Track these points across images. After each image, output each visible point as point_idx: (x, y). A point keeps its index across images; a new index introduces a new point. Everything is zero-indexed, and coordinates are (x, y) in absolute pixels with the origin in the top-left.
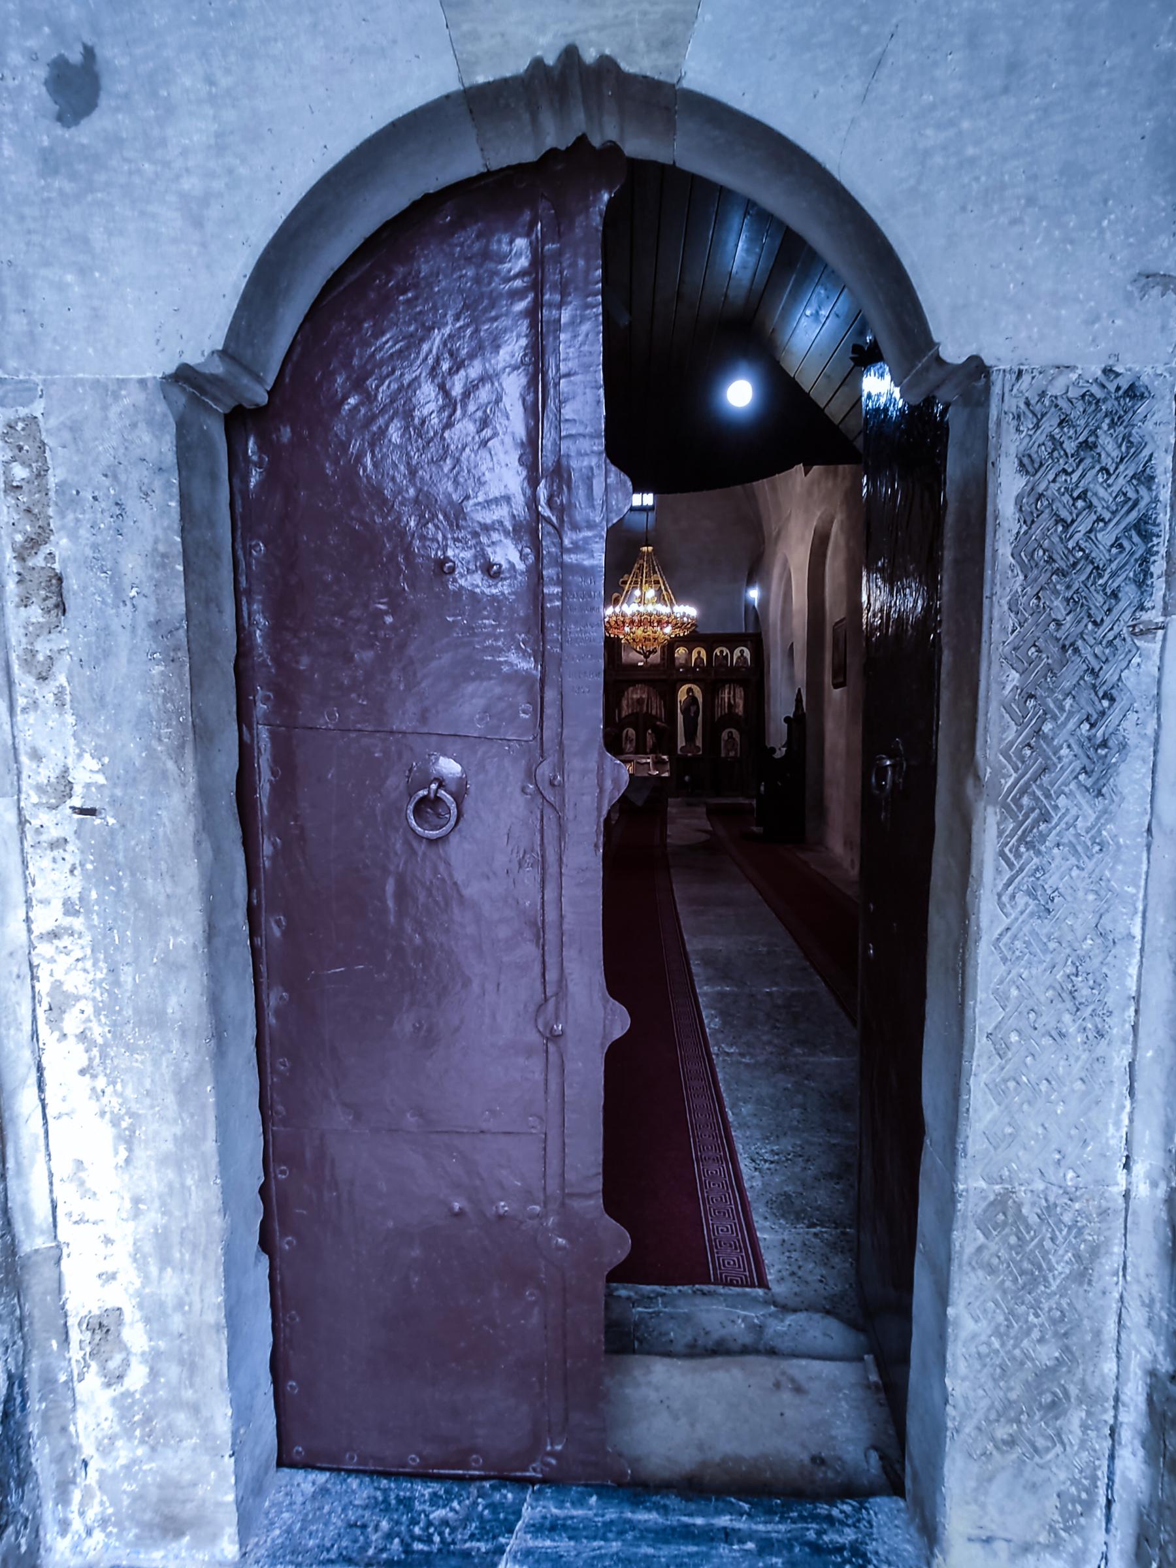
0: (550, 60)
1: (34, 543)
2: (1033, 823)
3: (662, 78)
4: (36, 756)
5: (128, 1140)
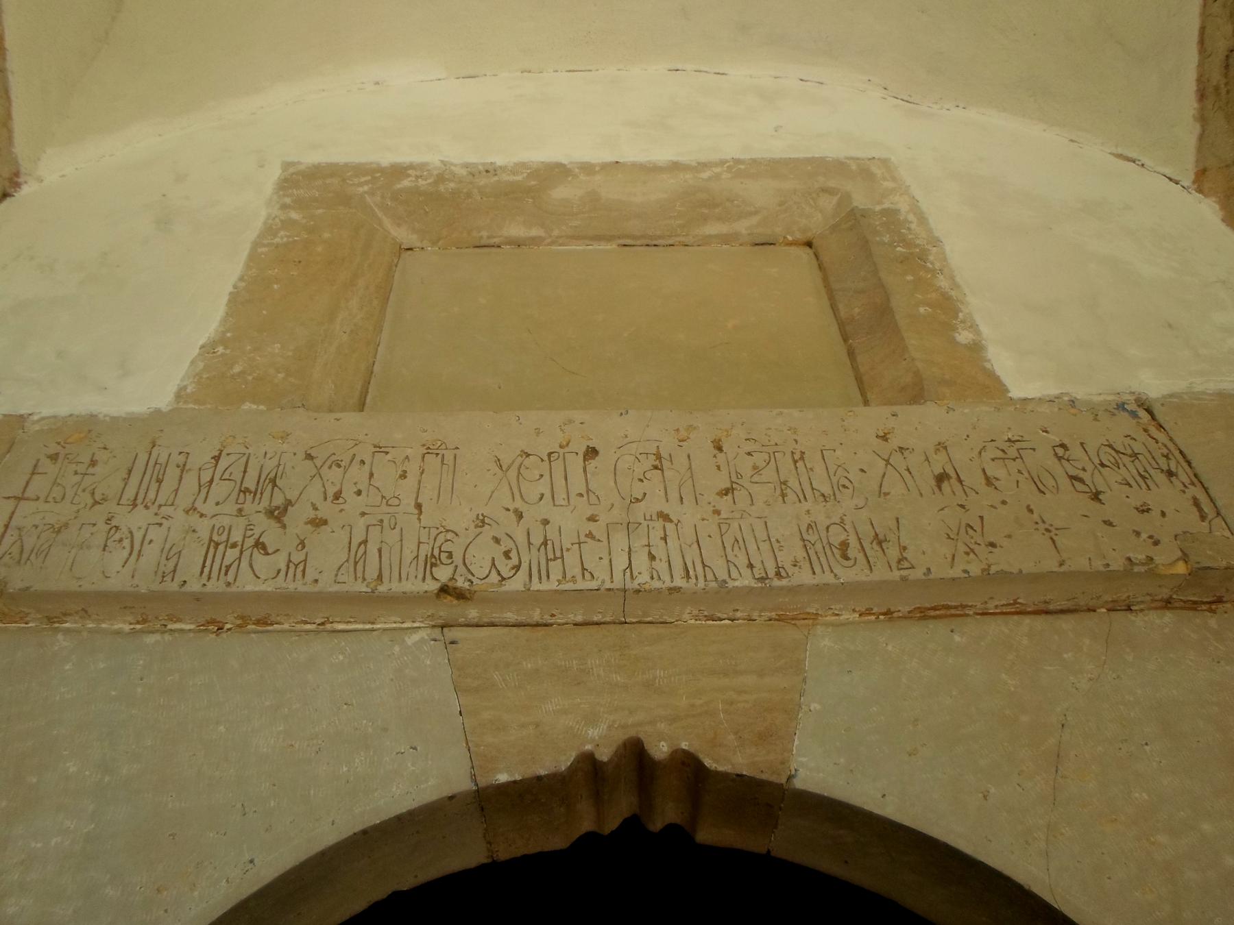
0: (604, 755)
3: (764, 777)
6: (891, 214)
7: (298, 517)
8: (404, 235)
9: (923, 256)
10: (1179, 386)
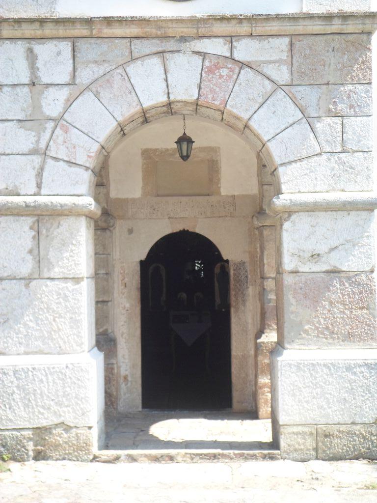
1: (123, 280)
2: (237, 311)
4: (122, 304)
5: (129, 352)
6: (217, 161)
7: (156, 210)
8: (157, 160)
9: (218, 170)
10: (238, 194)
